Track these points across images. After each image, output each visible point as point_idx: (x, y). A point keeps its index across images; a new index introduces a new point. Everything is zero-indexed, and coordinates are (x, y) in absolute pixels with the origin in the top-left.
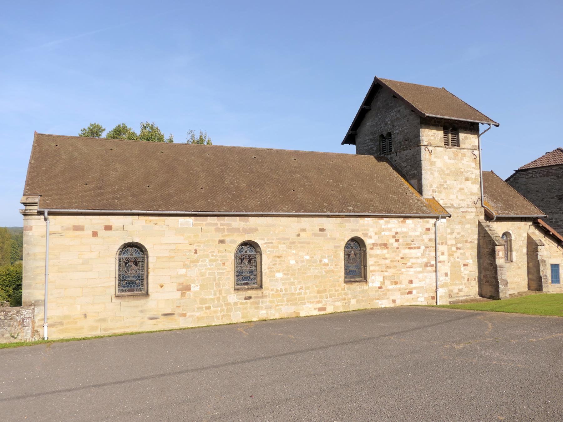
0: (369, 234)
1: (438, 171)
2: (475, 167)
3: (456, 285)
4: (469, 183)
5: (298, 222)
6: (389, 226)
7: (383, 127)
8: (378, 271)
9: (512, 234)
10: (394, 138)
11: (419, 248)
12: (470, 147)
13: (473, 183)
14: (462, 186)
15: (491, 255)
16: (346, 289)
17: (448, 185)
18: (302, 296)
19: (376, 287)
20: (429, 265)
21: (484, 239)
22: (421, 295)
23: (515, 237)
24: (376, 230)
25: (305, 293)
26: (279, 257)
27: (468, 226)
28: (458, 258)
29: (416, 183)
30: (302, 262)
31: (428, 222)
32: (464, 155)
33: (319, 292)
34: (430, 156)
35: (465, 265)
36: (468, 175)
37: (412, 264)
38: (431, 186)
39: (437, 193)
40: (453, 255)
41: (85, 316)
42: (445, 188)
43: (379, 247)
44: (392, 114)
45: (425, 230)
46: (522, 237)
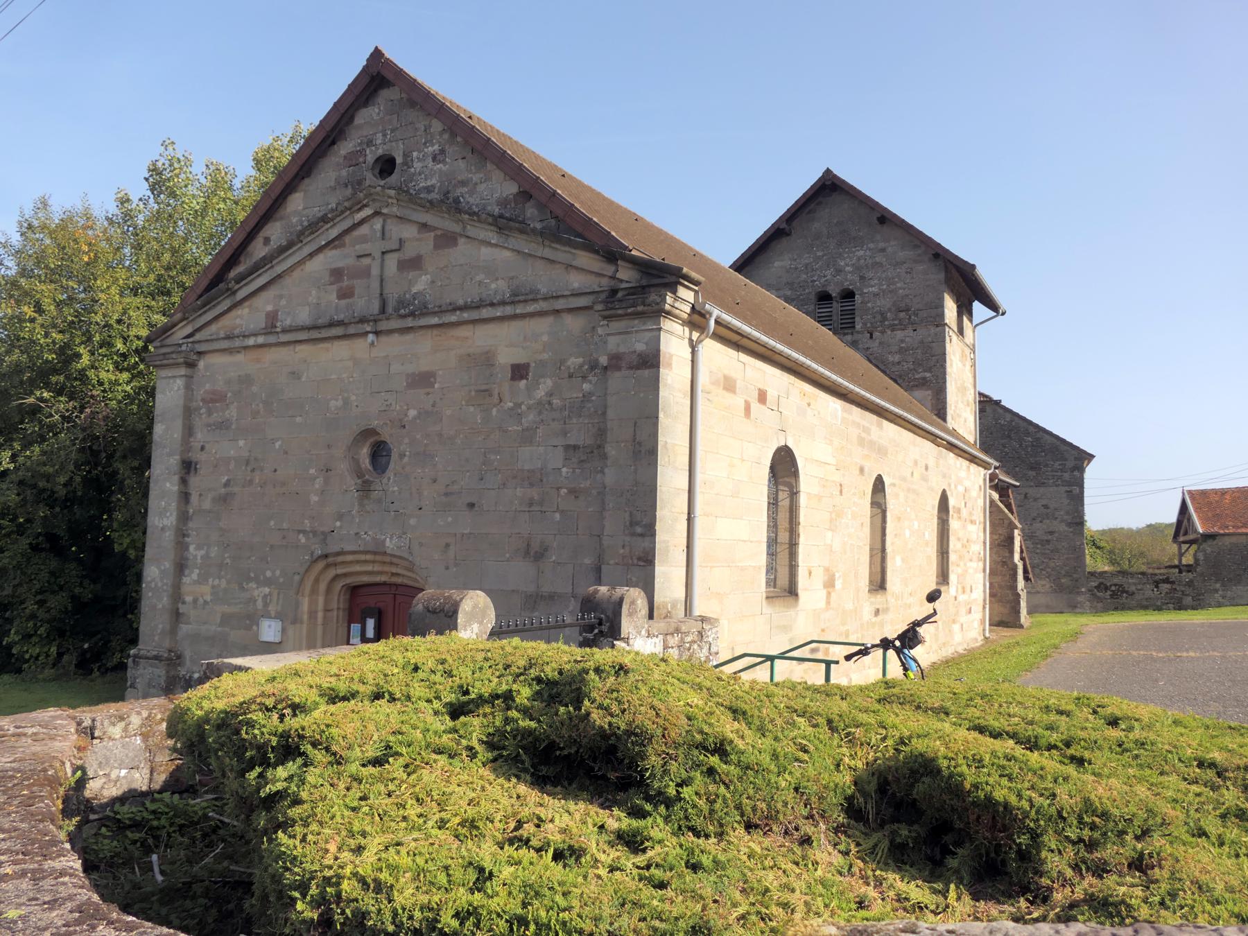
44: (861, 253)
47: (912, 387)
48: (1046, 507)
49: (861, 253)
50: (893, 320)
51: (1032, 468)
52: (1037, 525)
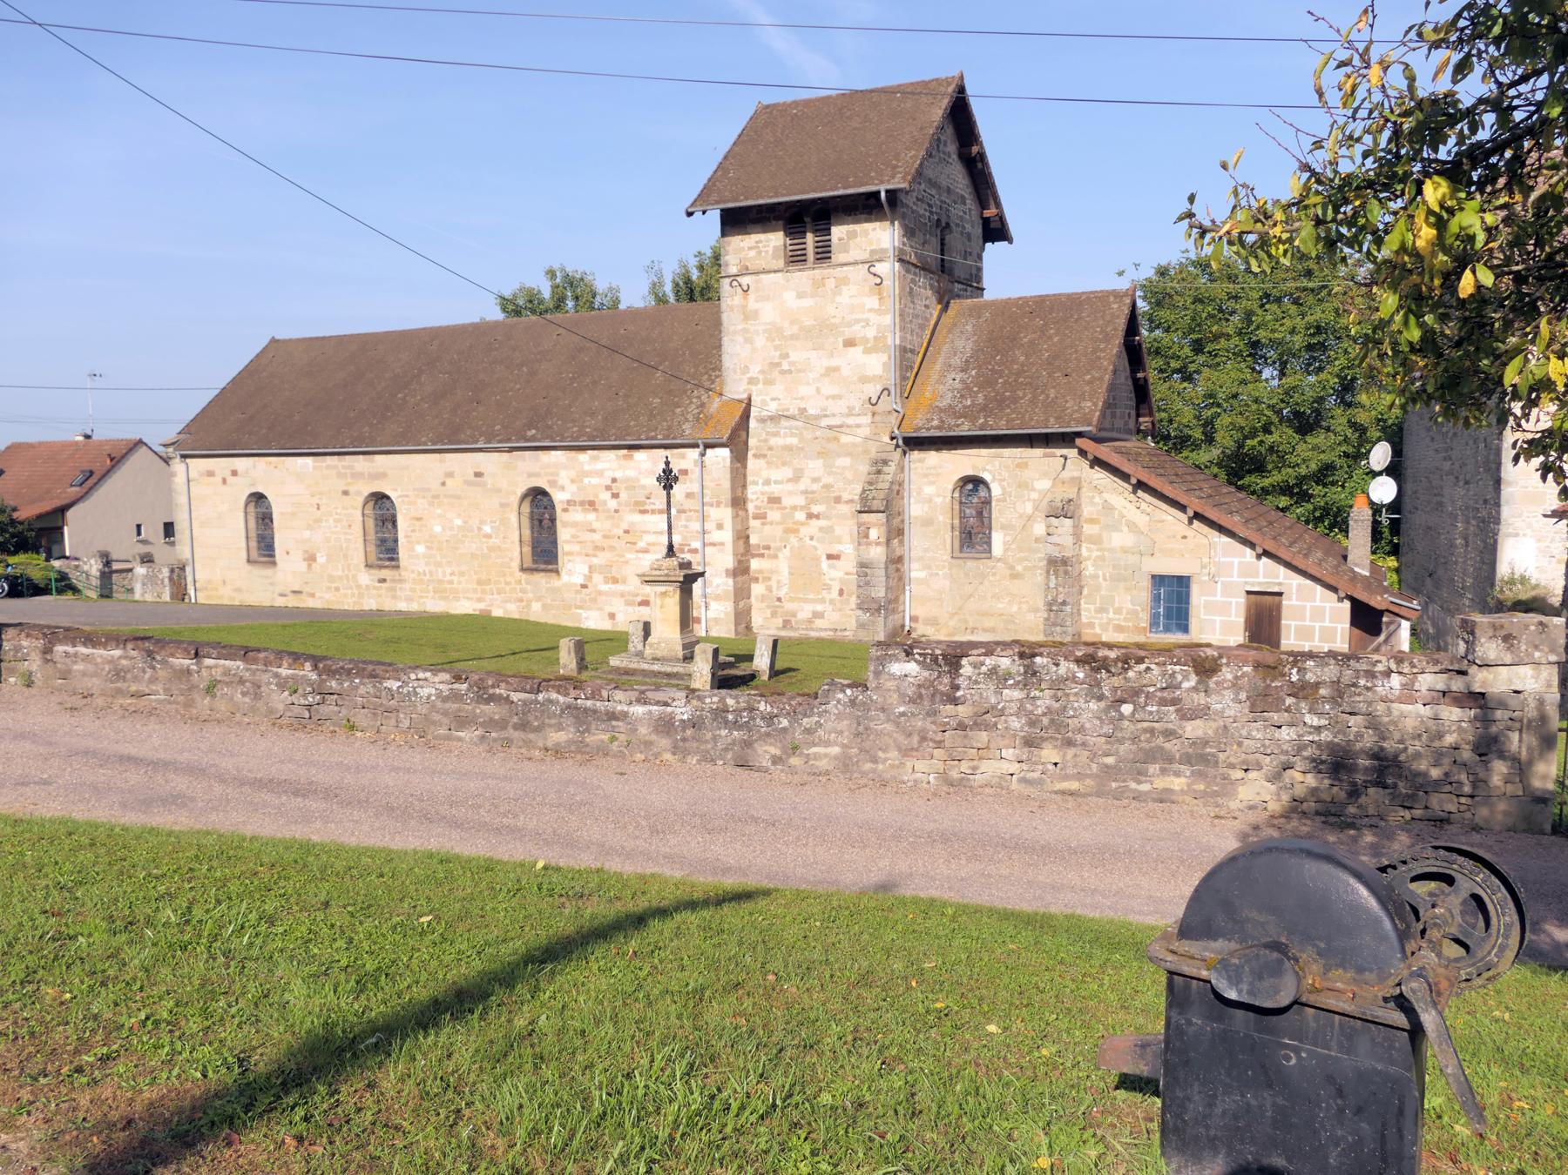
0: (560, 482)
1: (765, 331)
2: (877, 307)
3: (806, 601)
4: (855, 353)
5: (441, 461)
6: (599, 466)
8: (579, 554)
9: (993, 481)
12: (865, 256)
13: (867, 351)
14: (834, 362)
17: (792, 364)
18: (455, 586)
20: (686, 548)
23: (1003, 488)
24: (573, 474)
25: (460, 582)
26: (419, 519)
27: (845, 461)
28: (812, 538)
30: (451, 529)
31: (683, 457)
32: (842, 282)
33: (479, 582)
34: (745, 298)
35: (830, 557)
36: (857, 331)
38: (746, 369)
39: (760, 386)
40: (796, 531)
41: (224, 582)
42: (783, 372)
43: (580, 508)
46: (1033, 489)
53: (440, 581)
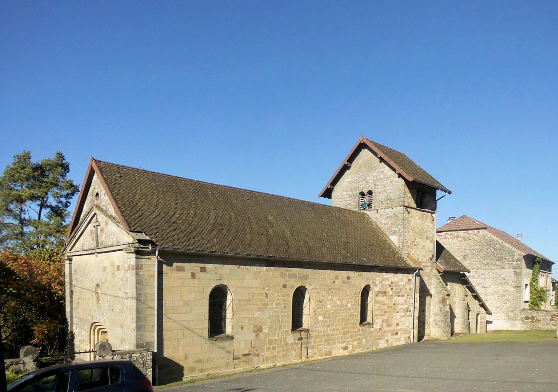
7: (364, 185)
8: (380, 315)
10: (375, 197)
11: (404, 296)
15: (441, 303)
16: (360, 331)
19: (377, 329)
20: (408, 310)
21: (436, 289)
22: (403, 335)
25: (336, 334)
26: (321, 302)
29: (397, 239)
37: (399, 309)
42: (415, 245)
43: (381, 295)
44: (375, 174)
45: (408, 281)
47: (392, 234)
48: (504, 279)
49: (375, 174)
50: (385, 204)
51: (499, 260)
52: (500, 288)
53: (328, 335)
